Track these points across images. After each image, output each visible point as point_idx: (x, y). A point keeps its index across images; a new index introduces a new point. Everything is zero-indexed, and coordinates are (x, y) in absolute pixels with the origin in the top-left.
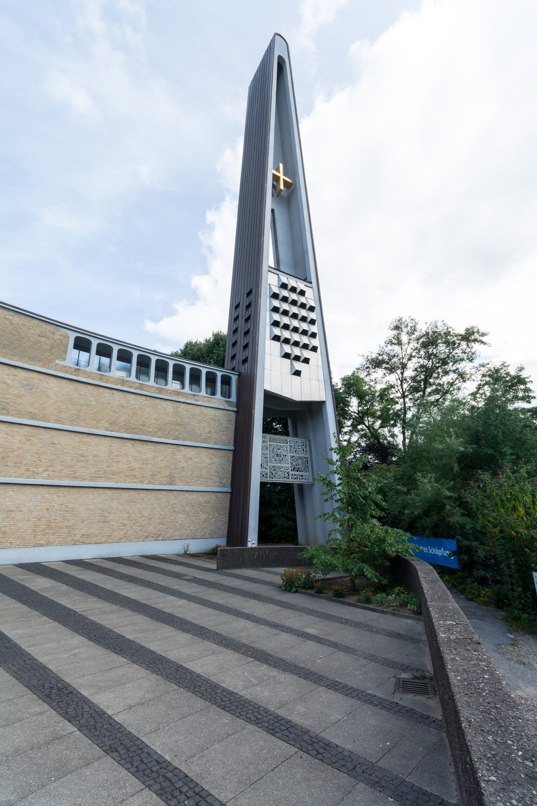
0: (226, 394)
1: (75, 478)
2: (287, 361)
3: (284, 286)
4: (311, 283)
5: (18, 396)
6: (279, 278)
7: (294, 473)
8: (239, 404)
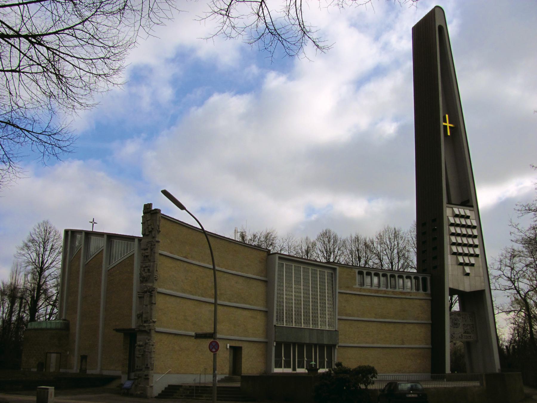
0: (425, 289)
1: (367, 343)
2: (461, 267)
3: (456, 216)
4: (472, 206)
5: (345, 307)
6: (453, 211)
7: (465, 335)
8: (432, 295)
